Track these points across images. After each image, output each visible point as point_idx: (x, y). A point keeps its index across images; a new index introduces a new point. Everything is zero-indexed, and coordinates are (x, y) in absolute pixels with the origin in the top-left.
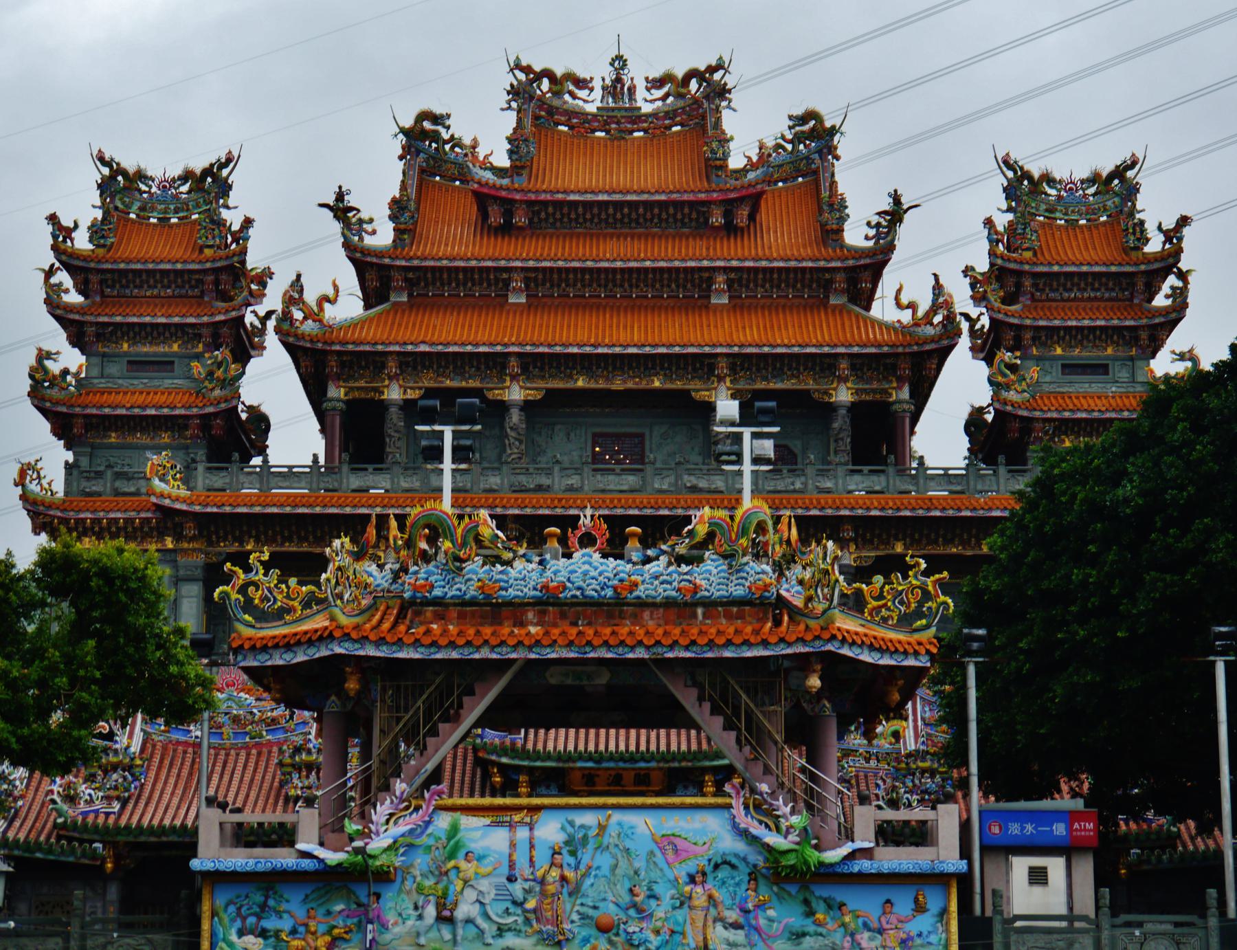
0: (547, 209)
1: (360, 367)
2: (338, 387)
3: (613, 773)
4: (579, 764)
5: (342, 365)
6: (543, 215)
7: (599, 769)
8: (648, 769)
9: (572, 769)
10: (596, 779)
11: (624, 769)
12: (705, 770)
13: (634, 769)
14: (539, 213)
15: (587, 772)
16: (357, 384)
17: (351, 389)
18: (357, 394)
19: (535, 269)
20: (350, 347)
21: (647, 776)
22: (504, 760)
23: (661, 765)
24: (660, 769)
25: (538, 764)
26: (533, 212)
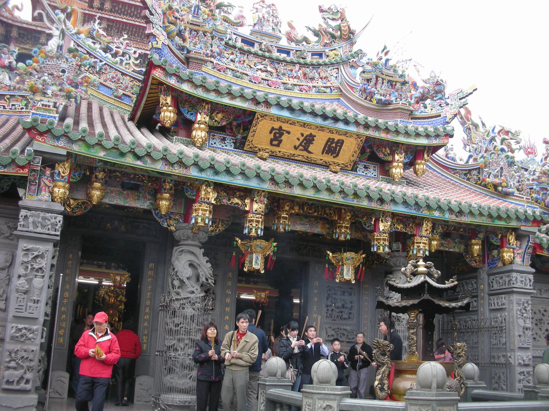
0: (119, 6)
1: (28, 39)
2: (16, 46)
3: (307, 132)
4: (274, 111)
5: (19, 34)
6: (117, 8)
7: (293, 123)
8: (346, 133)
9: (264, 116)
10: (285, 137)
11: (321, 128)
12: (395, 147)
13: (331, 131)
14: (115, 7)
15: (277, 125)
16: (25, 47)
17: (22, 48)
18: (24, 51)
19: (113, 21)
20: (25, 26)
21: (341, 143)
22: (186, 87)
23: (362, 131)
24: (358, 136)
25: (226, 101)
26: (113, 6)
